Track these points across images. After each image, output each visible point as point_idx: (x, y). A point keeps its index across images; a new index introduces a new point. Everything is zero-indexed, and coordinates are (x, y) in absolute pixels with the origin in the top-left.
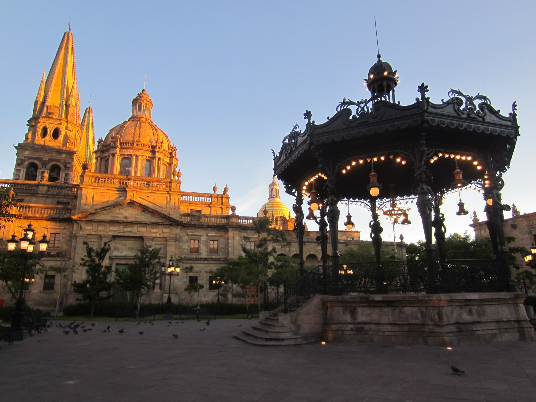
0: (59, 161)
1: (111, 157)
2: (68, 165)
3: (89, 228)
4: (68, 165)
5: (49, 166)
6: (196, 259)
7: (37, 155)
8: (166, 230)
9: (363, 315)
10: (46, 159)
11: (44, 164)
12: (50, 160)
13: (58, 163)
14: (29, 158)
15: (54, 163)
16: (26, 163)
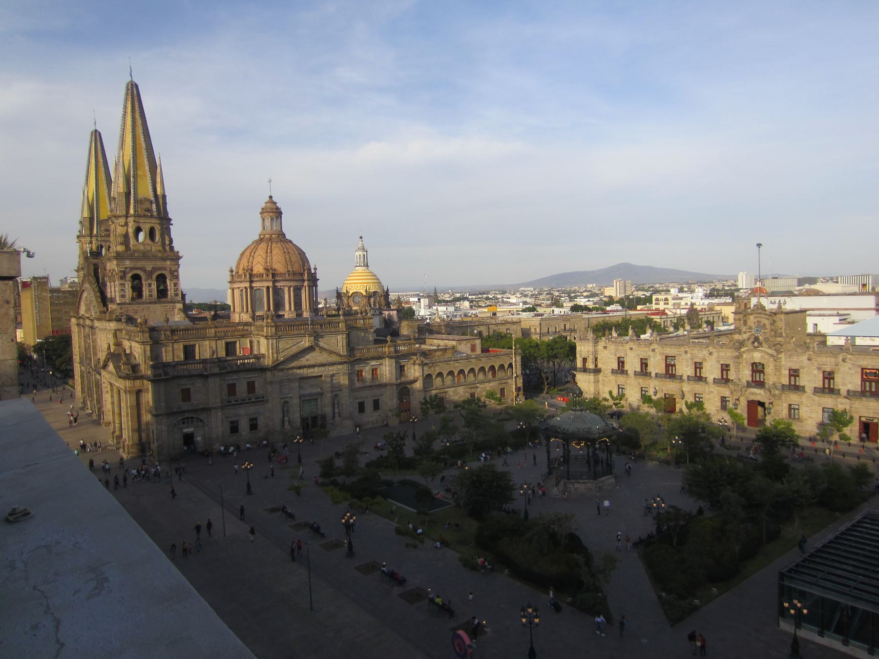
0: (165, 269)
1: (265, 289)
2: (175, 274)
3: (281, 374)
4: (175, 274)
5: (154, 276)
6: (364, 387)
7: (140, 264)
8: (340, 367)
9: (576, 485)
10: (149, 268)
11: (150, 274)
12: (154, 269)
13: (163, 272)
14: (132, 269)
15: (159, 272)
16: (130, 275)
